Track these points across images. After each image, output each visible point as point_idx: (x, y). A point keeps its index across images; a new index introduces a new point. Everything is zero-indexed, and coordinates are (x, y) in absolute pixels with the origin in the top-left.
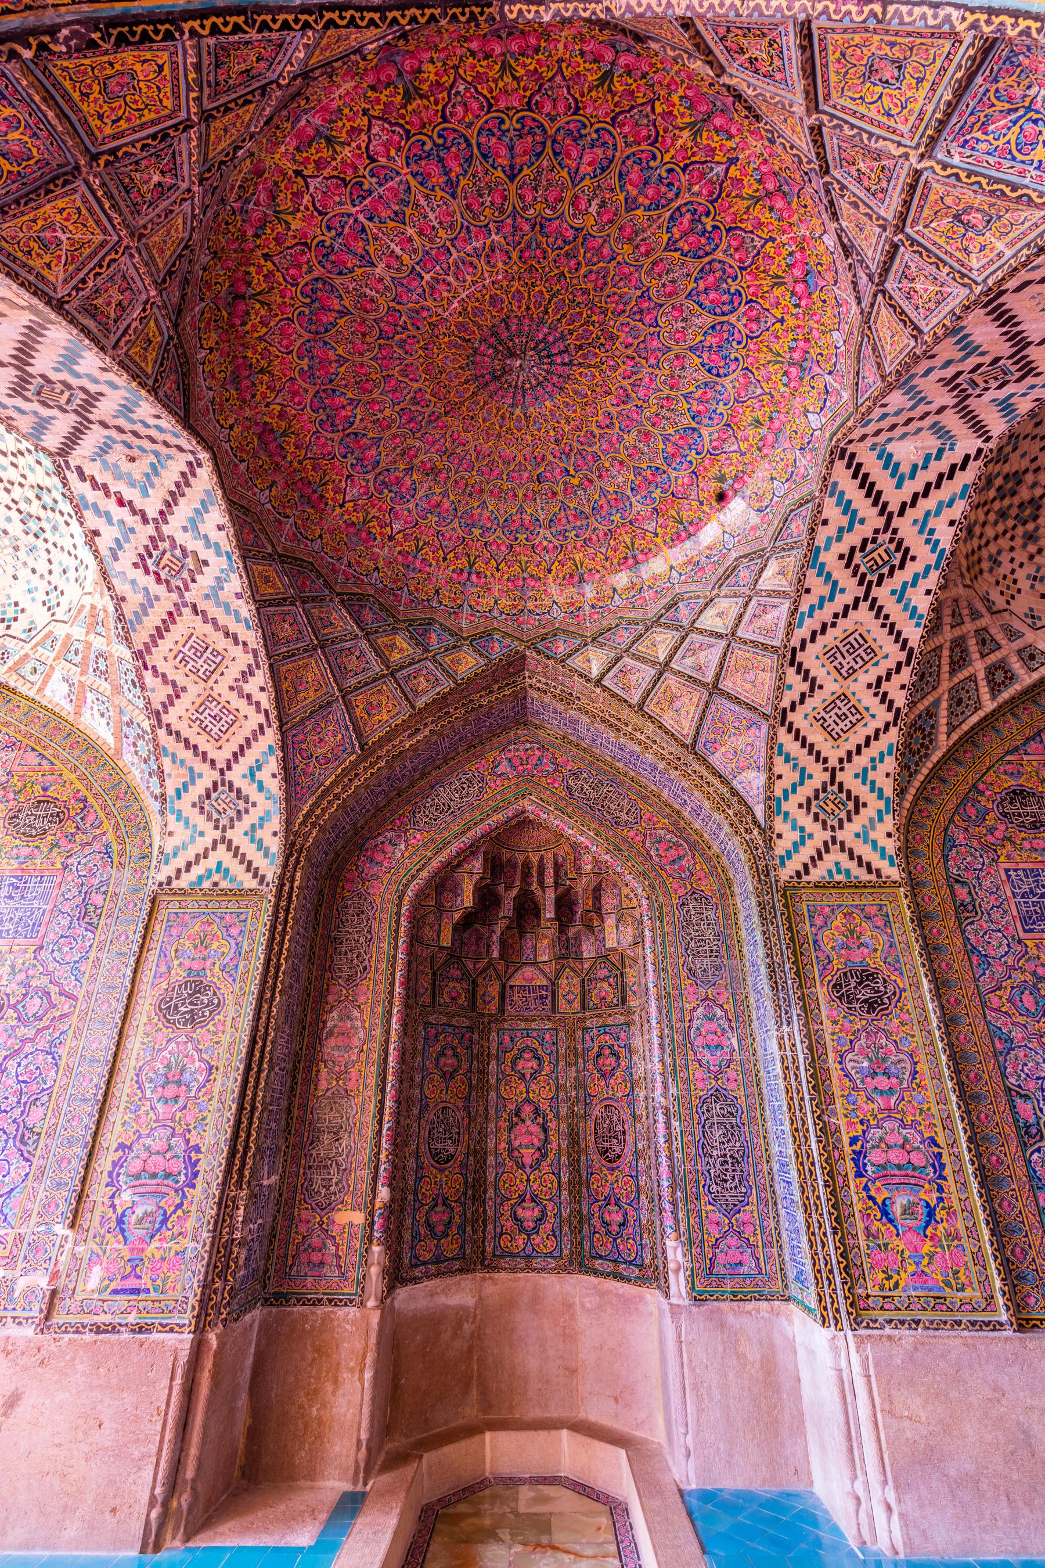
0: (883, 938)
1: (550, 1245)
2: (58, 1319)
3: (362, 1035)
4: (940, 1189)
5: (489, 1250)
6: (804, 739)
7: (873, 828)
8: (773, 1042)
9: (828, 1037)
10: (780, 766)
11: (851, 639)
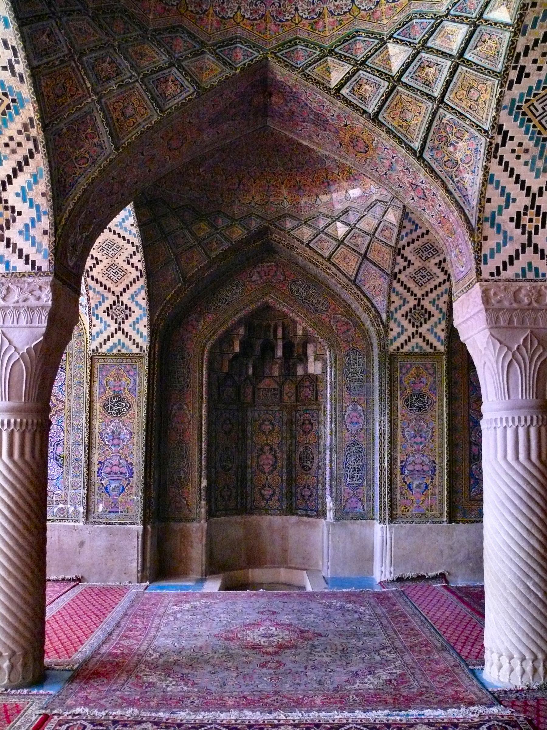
0: (431, 379)
1: (277, 504)
2: (91, 520)
3: (189, 417)
4: (432, 479)
5: (249, 506)
6: (405, 285)
7: (436, 326)
8: (379, 423)
9: (399, 422)
10: (394, 297)
11: (426, 245)
